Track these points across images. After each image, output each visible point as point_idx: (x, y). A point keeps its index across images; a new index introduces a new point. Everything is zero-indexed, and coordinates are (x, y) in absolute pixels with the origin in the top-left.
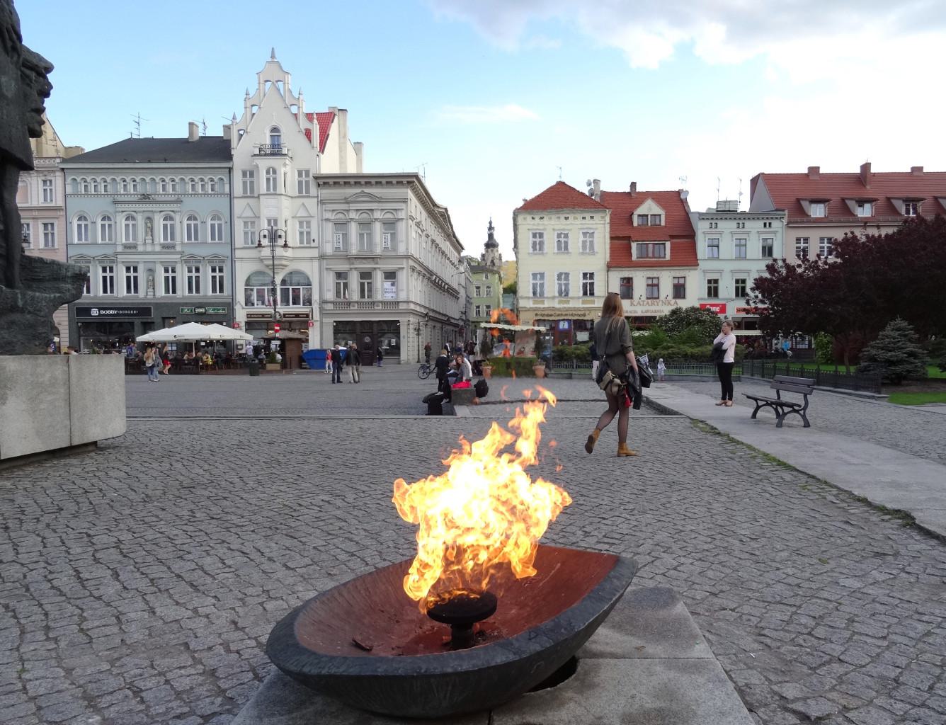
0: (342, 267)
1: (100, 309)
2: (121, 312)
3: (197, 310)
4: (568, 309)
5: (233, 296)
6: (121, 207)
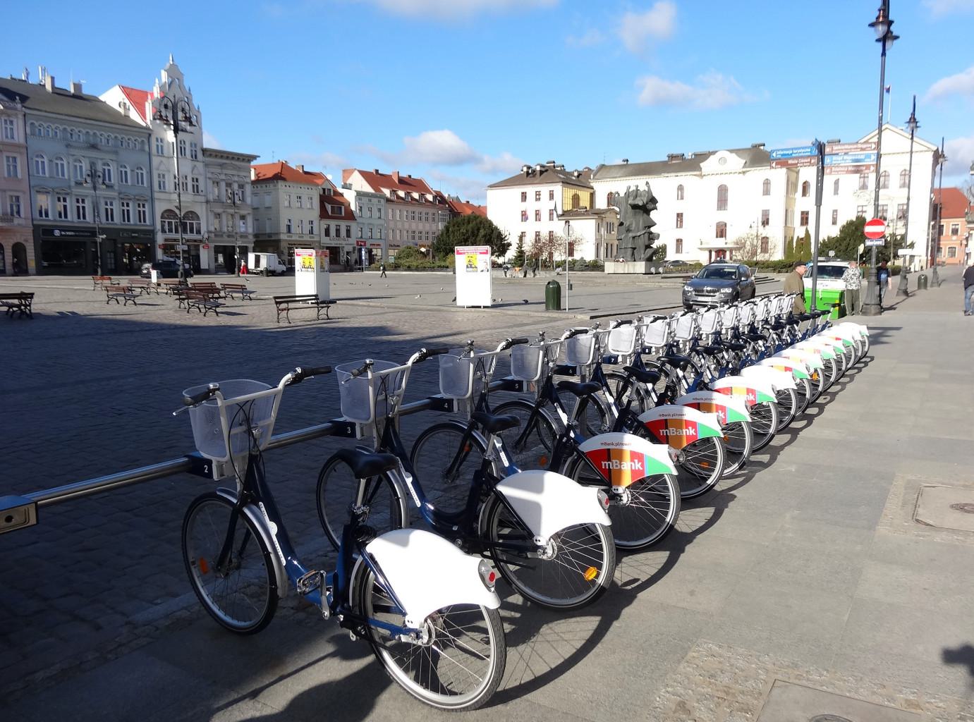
0: (219, 210)
1: (61, 231)
2: (77, 234)
3: (133, 235)
4: (302, 241)
5: (153, 224)
6: (73, 151)
